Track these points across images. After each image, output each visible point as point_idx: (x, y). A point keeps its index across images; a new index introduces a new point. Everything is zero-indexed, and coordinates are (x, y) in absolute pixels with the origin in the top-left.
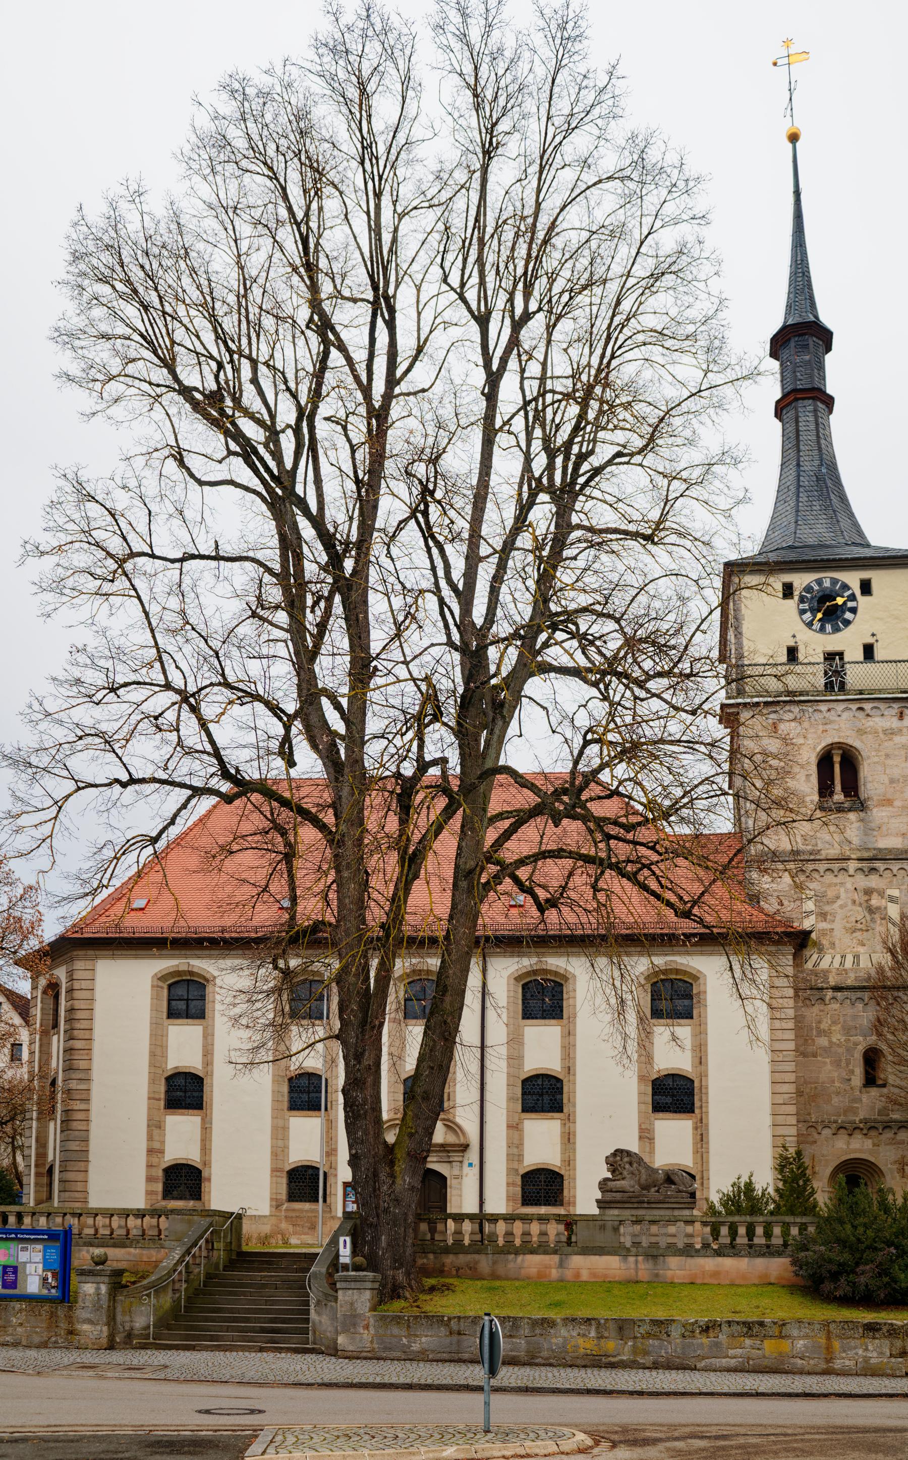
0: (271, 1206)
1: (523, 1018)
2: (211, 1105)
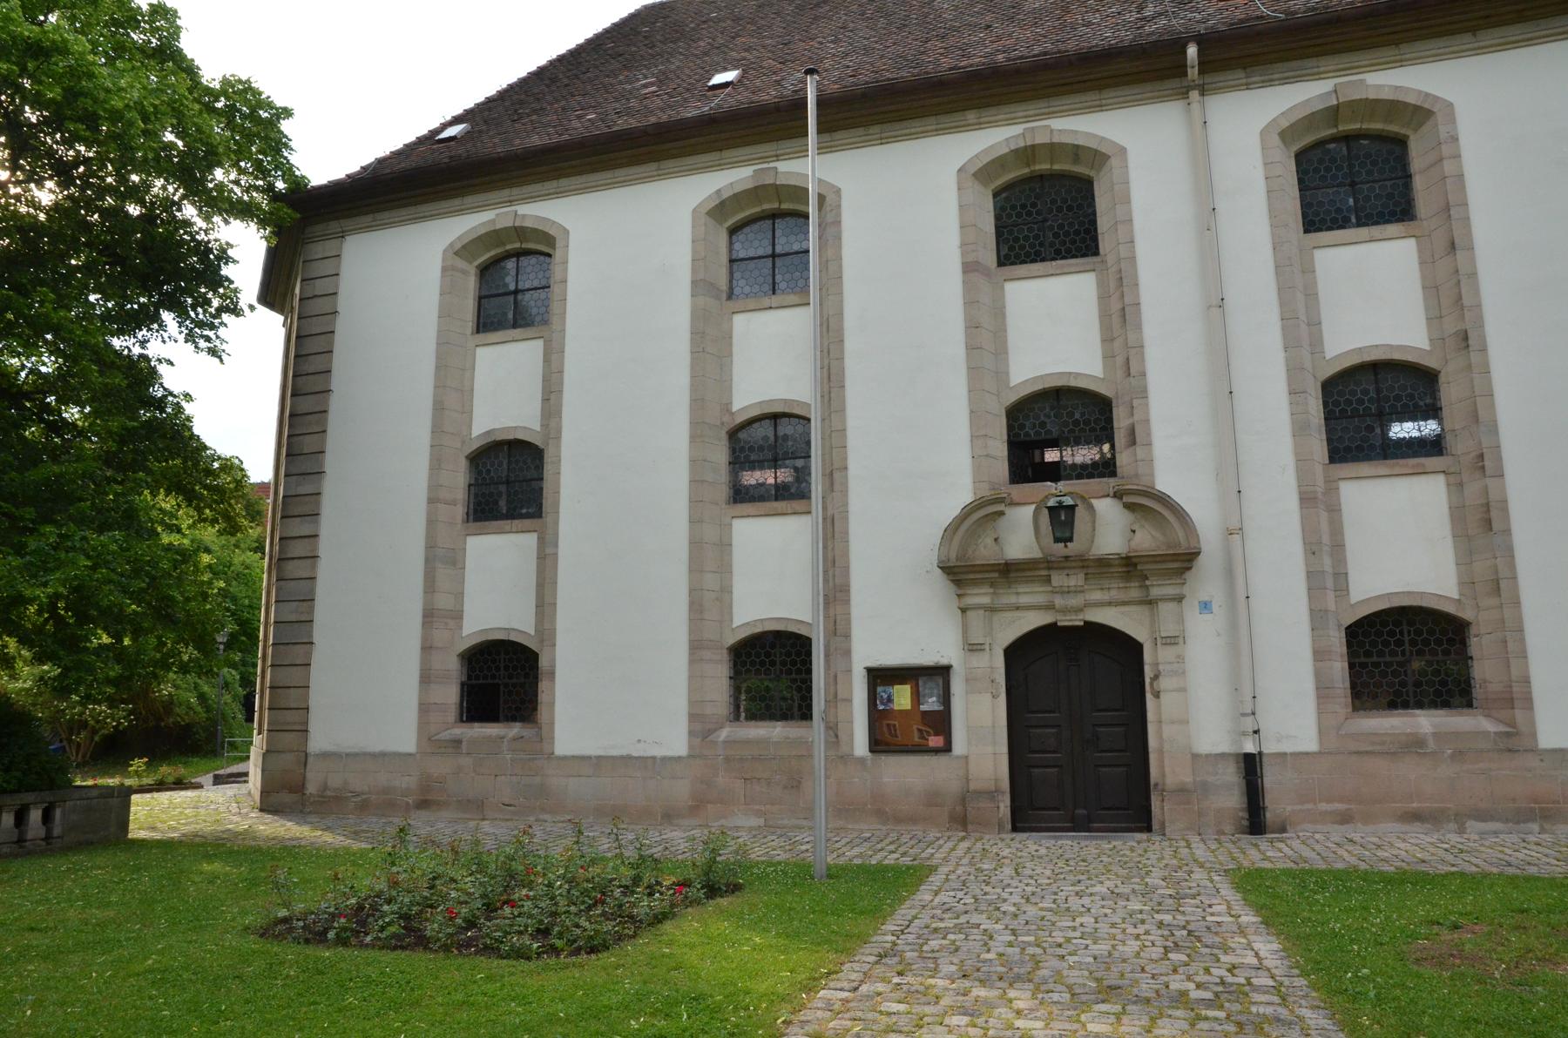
0: (691, 733)
1: (1306, 231)
2: (557, 504)
